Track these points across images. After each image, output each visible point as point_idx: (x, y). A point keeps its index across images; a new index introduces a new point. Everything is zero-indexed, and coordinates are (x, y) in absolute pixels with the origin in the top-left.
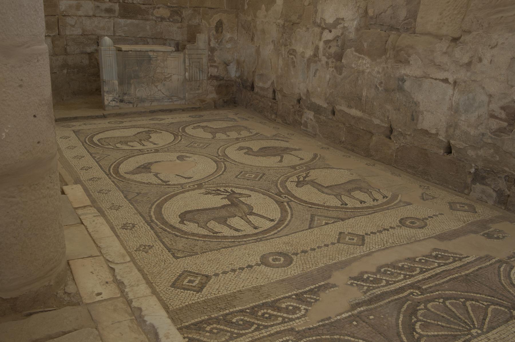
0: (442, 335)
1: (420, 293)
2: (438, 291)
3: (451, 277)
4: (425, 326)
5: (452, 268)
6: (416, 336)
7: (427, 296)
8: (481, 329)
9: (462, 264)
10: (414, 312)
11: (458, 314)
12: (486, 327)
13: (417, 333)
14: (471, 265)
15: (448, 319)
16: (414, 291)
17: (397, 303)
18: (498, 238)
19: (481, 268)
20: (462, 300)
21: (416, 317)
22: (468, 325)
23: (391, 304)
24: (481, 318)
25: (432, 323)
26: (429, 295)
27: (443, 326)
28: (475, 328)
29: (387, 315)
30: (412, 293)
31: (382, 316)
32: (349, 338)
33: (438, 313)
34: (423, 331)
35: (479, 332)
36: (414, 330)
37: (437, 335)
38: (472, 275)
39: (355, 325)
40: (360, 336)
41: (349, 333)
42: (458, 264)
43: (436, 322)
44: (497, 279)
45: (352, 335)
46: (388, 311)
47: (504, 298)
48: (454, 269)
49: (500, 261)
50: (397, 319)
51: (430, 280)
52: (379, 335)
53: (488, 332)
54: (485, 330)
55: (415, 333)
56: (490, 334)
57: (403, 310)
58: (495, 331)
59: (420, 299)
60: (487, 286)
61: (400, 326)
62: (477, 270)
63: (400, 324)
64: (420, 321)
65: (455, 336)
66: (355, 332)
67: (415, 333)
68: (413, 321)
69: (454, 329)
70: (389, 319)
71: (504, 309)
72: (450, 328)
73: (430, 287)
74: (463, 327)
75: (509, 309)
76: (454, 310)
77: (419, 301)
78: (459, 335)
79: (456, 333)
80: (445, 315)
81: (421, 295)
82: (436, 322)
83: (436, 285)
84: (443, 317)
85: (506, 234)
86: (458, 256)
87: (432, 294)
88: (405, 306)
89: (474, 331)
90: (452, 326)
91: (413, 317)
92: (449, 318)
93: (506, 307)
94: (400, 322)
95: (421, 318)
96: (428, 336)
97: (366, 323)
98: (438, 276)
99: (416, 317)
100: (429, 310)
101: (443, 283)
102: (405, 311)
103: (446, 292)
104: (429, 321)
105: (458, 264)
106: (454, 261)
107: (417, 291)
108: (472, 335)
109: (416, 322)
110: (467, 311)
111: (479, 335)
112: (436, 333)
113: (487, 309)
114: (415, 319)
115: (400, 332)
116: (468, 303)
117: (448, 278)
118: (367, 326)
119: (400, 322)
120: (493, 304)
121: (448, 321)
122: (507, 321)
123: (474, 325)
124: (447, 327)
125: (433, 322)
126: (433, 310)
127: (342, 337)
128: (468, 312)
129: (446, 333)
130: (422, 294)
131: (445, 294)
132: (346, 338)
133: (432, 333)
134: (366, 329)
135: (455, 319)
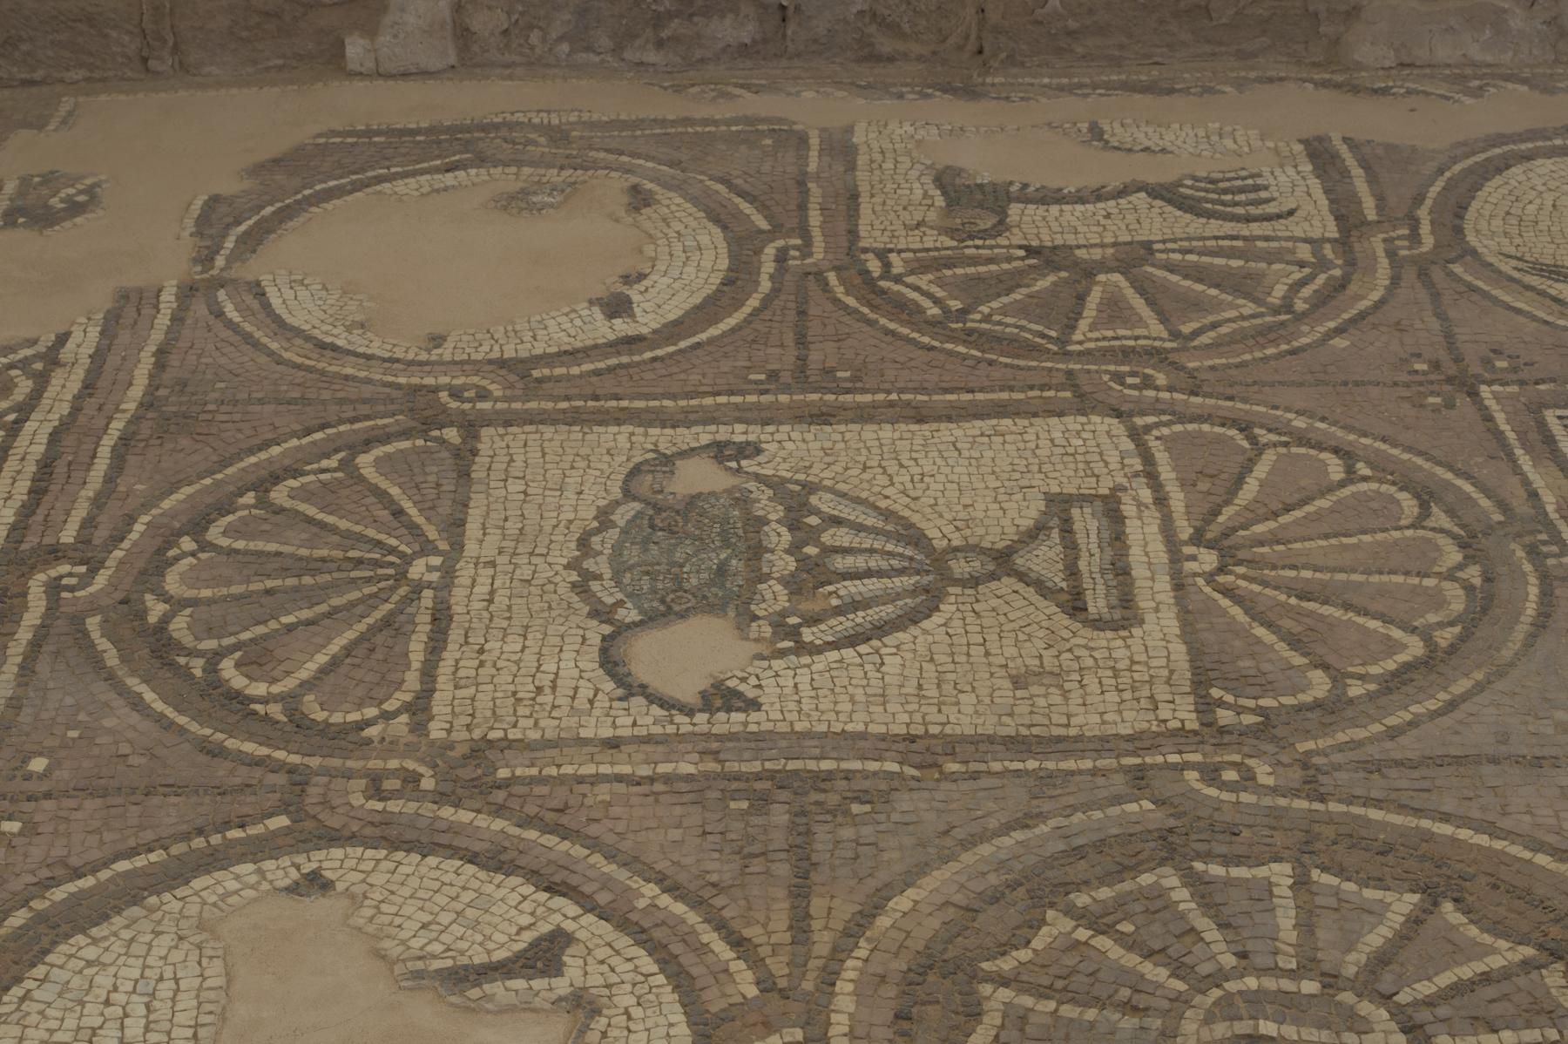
0: (348, 650)
1: (83, 569)
2: (131, 520)
3: (108, 442)
4: (257, 659)
5: (65, 409)
6: (275, 710)
7: (121, 562)
8: (427, 549)
9: (79, 374)
10: (161, 646)
11: (304, 552)
12: (432, 533)
13: (265, 701)
14: (112, 360)
15: (296, 589)
16: (53, 573)
17: (57, 653)
18: (75, 209)
19: (161, 353)
20: (249, 499)
21: (192, 653)
22: (376, 564)
23: (43, 666)
24: (384, 515)
25: (265, 637)
26: (118, 554)
27: (309, 623)
28: (407, 560)
29: (82, 717)
30: (54, 589)
31: (73, 734)
32: (71, 887)
33: (236, 589)
34: (274, 681)
35: (436, 561)
36: (237, 696)
37: (335, 663)
38: (162, 392)
39: (21, 833)
40: (95, 855)
41: (45, 873)
42: (64, 387)
43: (273, 625)
44: (263, 359)
45: (59, 872)
46: (69, 701)
47: (364, 410)
48: (76, 409)
49: (188, 291)
50: (137, 704)
51: (47, 499)
52: (156, 800)
53: (458, 546)
54: (443, 546)
55: (258, 707)
56: (471, 548)
57: (112, 659)
58: (473, 528)
59: (113, 585)
60: (261, 402)
61: (182, 720)
62: (160, 364)
63: (170, 712)
64: (219, 655)
65: (387, 622)
66: (58, 852)
67: (258, 707)
68: (198, 673)
69: (353, 604)
70: (109, 723)
71: (406, 444)
72: (335, 610)
73: (89, 523)
74: (368, 580)
75: (424, 434)
76: (272, 547)
77: (119, 596)
78: (391, 613)
79: (378, 615)
80: (270, 584)
81: (93, 572)
82: (273, 625)
83: (98, 502)
84: (268, 592)
85: (83, 177)
86: (28, 352)
87: (126, 544)
88: (103, 644)
89: (417, 570)
90: (336, 601)
91: (182, 660)
92: (291, 582)
93: (406, 434)
94: (159, 706)
95: (210, 644)
96: (307, 686)
97: (48, 795)
98: (60, 468)
99: (192, 653)
100: (194, 602)
101: (109, 479)
102: (123, 660)
103: (166, 504)
104: (246, 636)
105: (64, 387)
106: (42, 380)
107: (65, 568)
108: (429, 585)
109: (212, 667)
110: (310, 521)
111: (449, 572)
112: (322, 659)
113: (362, 479)
114: (200, 662)
115: (206, 738)
116: (279, 495)
117: (104, 452)
118: (72, 803)
119: (159, 706)
120: (368, 444)
121: (310, 597)
122: (464, 475)
123: (392, 551)
124: (328, 615)
125: (260, 630)
126: (206, 593)
127: (38, 905)
128: (323, 525)
129: (350, 635)
130: (94, 568)
131: (172, 514)
132: (59, 894)
133: (312, 666)
134: (79, 815)
135: (313, 572)
